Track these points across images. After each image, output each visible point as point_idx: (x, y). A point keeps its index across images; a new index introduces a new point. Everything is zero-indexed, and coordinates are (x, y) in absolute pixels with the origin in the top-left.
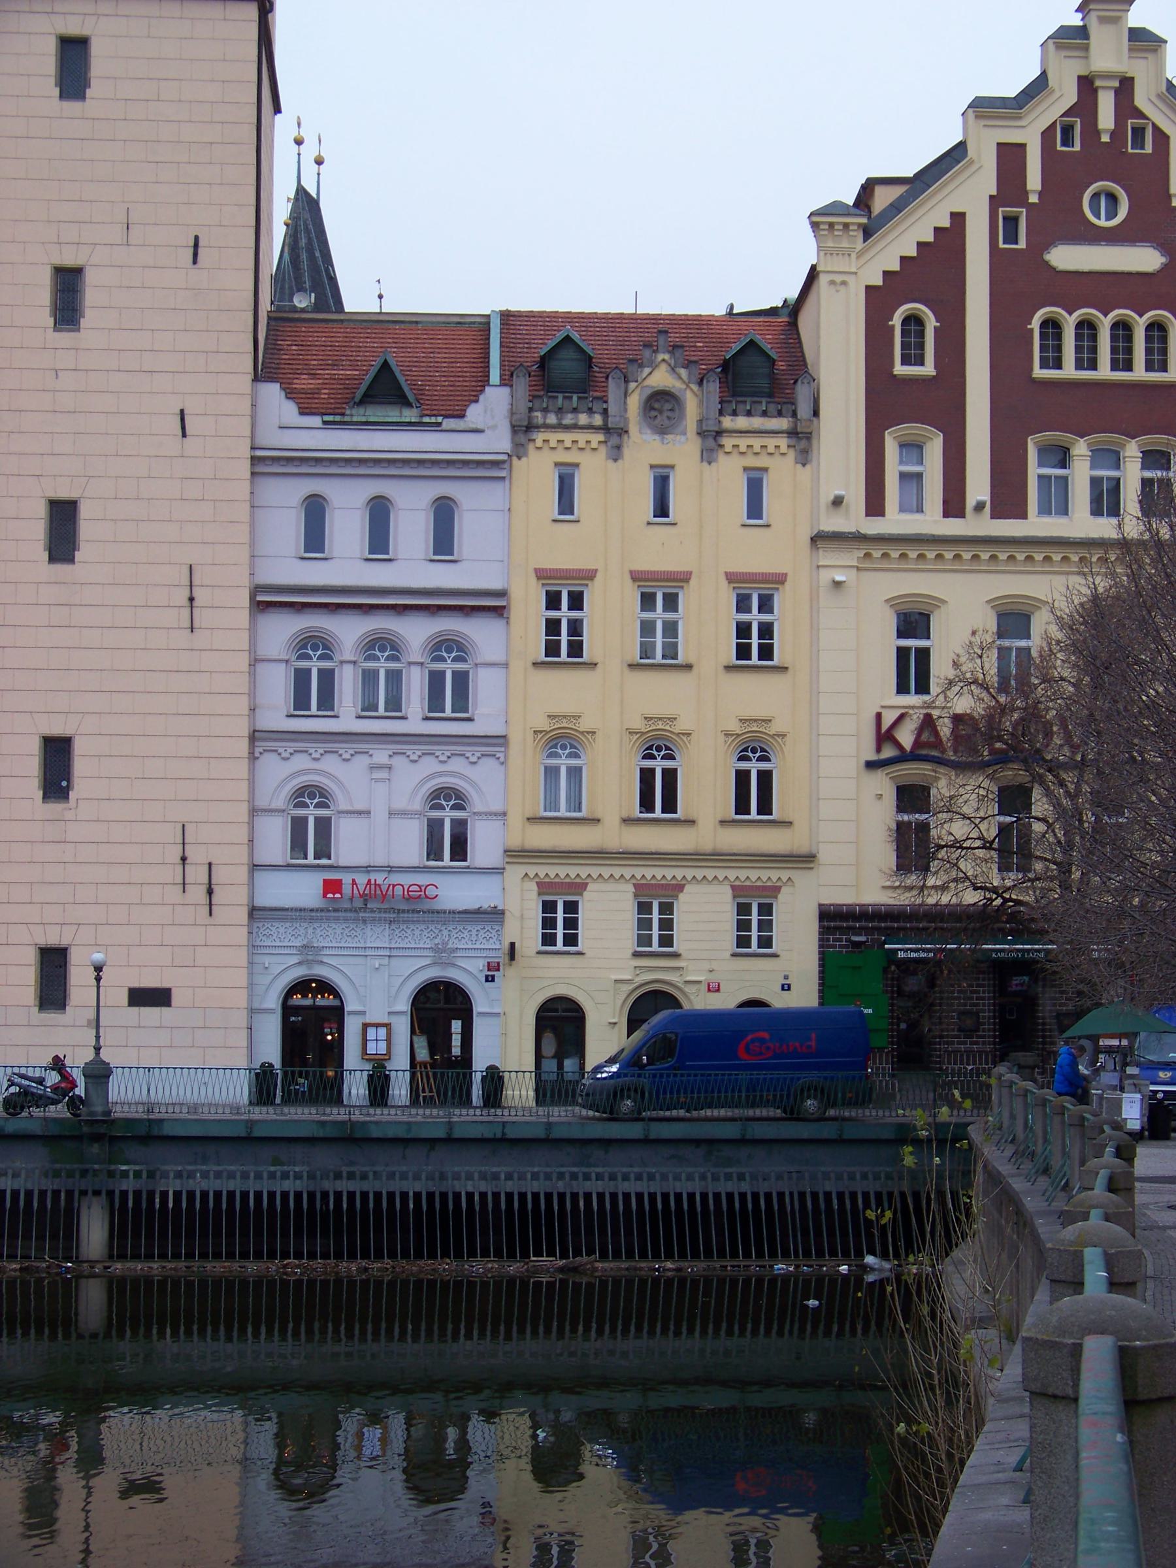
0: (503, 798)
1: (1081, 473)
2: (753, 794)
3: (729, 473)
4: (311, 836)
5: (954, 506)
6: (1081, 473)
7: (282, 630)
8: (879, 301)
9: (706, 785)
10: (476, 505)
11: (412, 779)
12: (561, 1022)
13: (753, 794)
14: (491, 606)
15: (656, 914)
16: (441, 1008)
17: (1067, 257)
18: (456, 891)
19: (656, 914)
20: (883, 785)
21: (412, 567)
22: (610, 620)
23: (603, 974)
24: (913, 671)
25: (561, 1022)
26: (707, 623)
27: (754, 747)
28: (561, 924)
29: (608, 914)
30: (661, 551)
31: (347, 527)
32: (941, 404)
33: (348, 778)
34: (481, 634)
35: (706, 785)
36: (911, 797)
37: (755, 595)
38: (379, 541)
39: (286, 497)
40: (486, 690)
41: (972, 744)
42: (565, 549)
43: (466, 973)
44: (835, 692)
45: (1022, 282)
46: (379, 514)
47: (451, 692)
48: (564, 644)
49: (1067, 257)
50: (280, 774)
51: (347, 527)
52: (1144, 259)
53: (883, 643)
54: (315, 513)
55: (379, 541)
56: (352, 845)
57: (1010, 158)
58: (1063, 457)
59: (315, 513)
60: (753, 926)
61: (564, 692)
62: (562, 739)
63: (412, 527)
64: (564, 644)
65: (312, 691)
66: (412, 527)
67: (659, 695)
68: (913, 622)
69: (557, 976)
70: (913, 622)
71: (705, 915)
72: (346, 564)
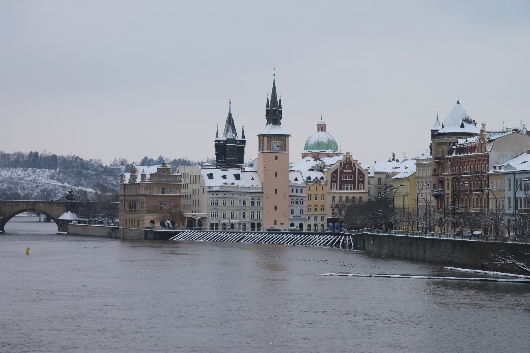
0: (305, 209)
1: (346, 187)
2: (322, 210)
3: (321, 187)
4: (292, 213)
5: (337, 189)
6: (346, 187)
7: (291, 198)
8: (332, 174)
9: (319, 209)
10: (304, 190)
11: (299, 209)
12: (309, 226)
13: (322, 210)
14: (305, 197)
15: (316, 219)
16: (301, 225)
17: (345, 171)
18: (302, 217)
19: (316, 219)
20: (331, 209)
21: (299, 194)
22: (313, 197)
23: (312, 223)
24: (334, 201)
25: (309, 226)
26: (319, 197)
27: (323, 206)
28: (309, 219)
29: (312, 218)
30: (316, 192)
31: (295, 191)
32: (336, 182)
33: (295, 209)
34: (304, 199)
35: (319, 209)
36: (333, 210)
37: (322, 195)
38: (297, 192)
39: (291, 189)
40: (304, 202)
41: (337, 206)
42: (310, 192)
43: (303, 222)
44: (328, 202)
45: (342, 173)
46: (297, 190)
47: (302, 203)
48: (310, 199)
49: (345, 171)
50: (291, 208)
51: (295, 191)
52: (350, 171)
53: (332, 199)
54: (292, 190)
55: (297, 192)
56: (295, 213)
57: (341, 163)
58: (344, 185)
59: (292, 190)
60: (322, 219)
61: (310, 203)
62: (309, 206)
63: (299, 191)
64: (310, 199)
65: (292, 202)
66: (299, 191)
67: (316, 203)
68: (334, 197)
69: (309, 223)
70: (334, 197)
71: (319, 218)
72: (295, 194)
